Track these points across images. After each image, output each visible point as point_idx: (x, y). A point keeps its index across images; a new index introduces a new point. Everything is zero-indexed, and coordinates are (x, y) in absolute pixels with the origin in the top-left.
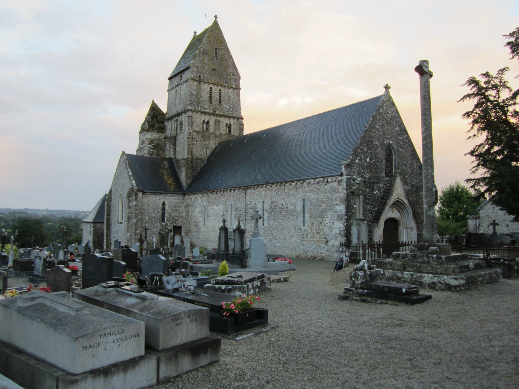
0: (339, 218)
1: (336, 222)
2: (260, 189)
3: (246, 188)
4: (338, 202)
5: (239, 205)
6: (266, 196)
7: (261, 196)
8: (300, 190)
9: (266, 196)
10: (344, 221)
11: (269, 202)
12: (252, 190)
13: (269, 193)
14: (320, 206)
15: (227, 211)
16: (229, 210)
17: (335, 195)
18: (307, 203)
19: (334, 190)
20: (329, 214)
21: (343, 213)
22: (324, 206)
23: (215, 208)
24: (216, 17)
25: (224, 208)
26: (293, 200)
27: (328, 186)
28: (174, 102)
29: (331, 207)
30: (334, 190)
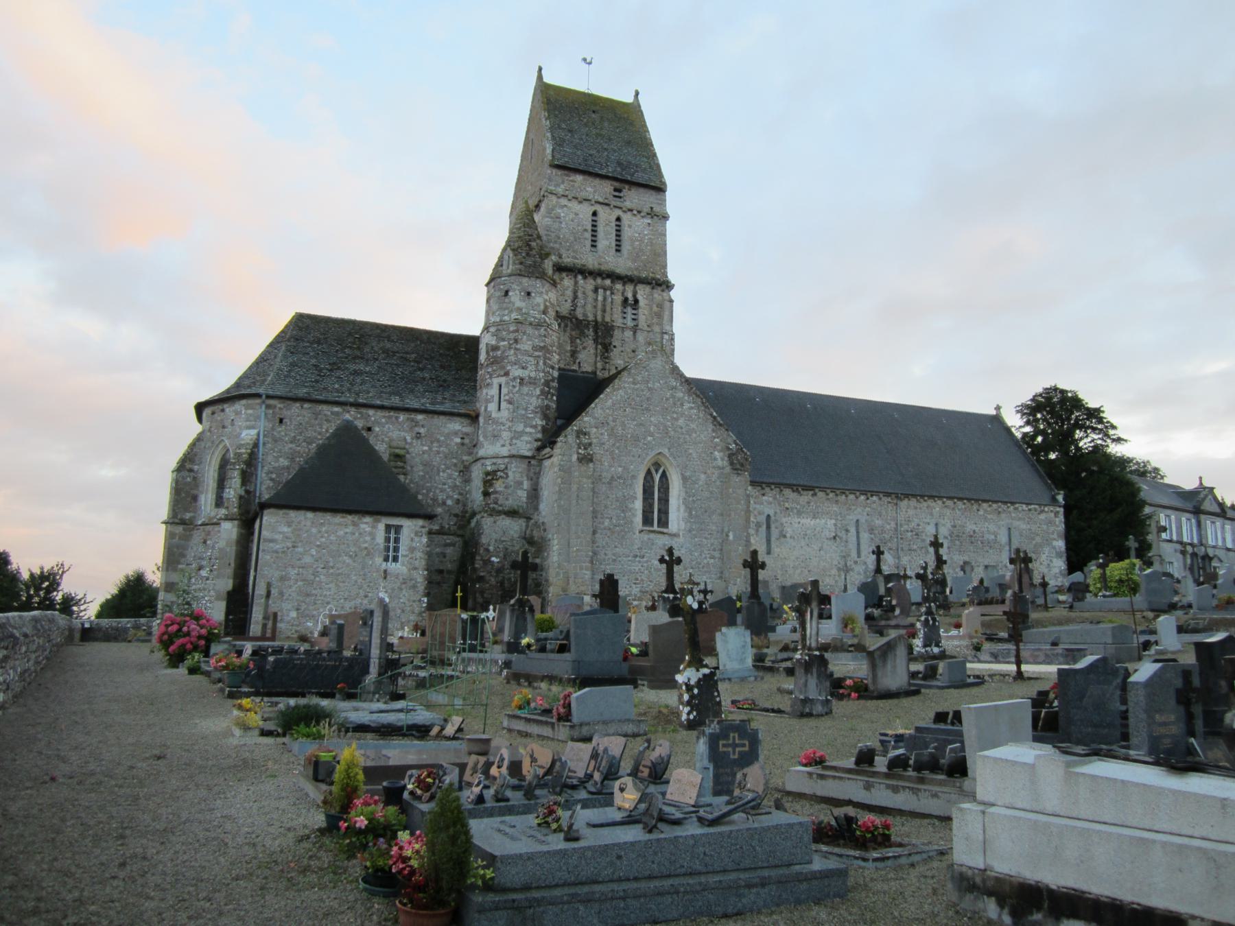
0: (1059, 555)
1: (1054, 560)
2: (931, 503)
3: (900, 496)
4: (1055, 536)
5: (878, 522)
6: (942, 515)
7: (931, 514)
8: (1003, 516)
9: (942, 515)
10: (1064, 558)
11: (949, 525)
12: (913, 502)
13: (948, 512)
14: (1033, 539)
15: (847, 531)
16: (853, 530)
17: (1052, 529)
18: (1015, 534)
19: (1050, 522)
20: (1046, 550)
21: (1063, 548)
22: (1038, 539)
23: (808, 522)
24: (637, 94)
25: (835, 525)
26: (992, 527)
27: (1042, 516)
28: (588, 235)
29: (1048, 542)
30: (1050, 522)
